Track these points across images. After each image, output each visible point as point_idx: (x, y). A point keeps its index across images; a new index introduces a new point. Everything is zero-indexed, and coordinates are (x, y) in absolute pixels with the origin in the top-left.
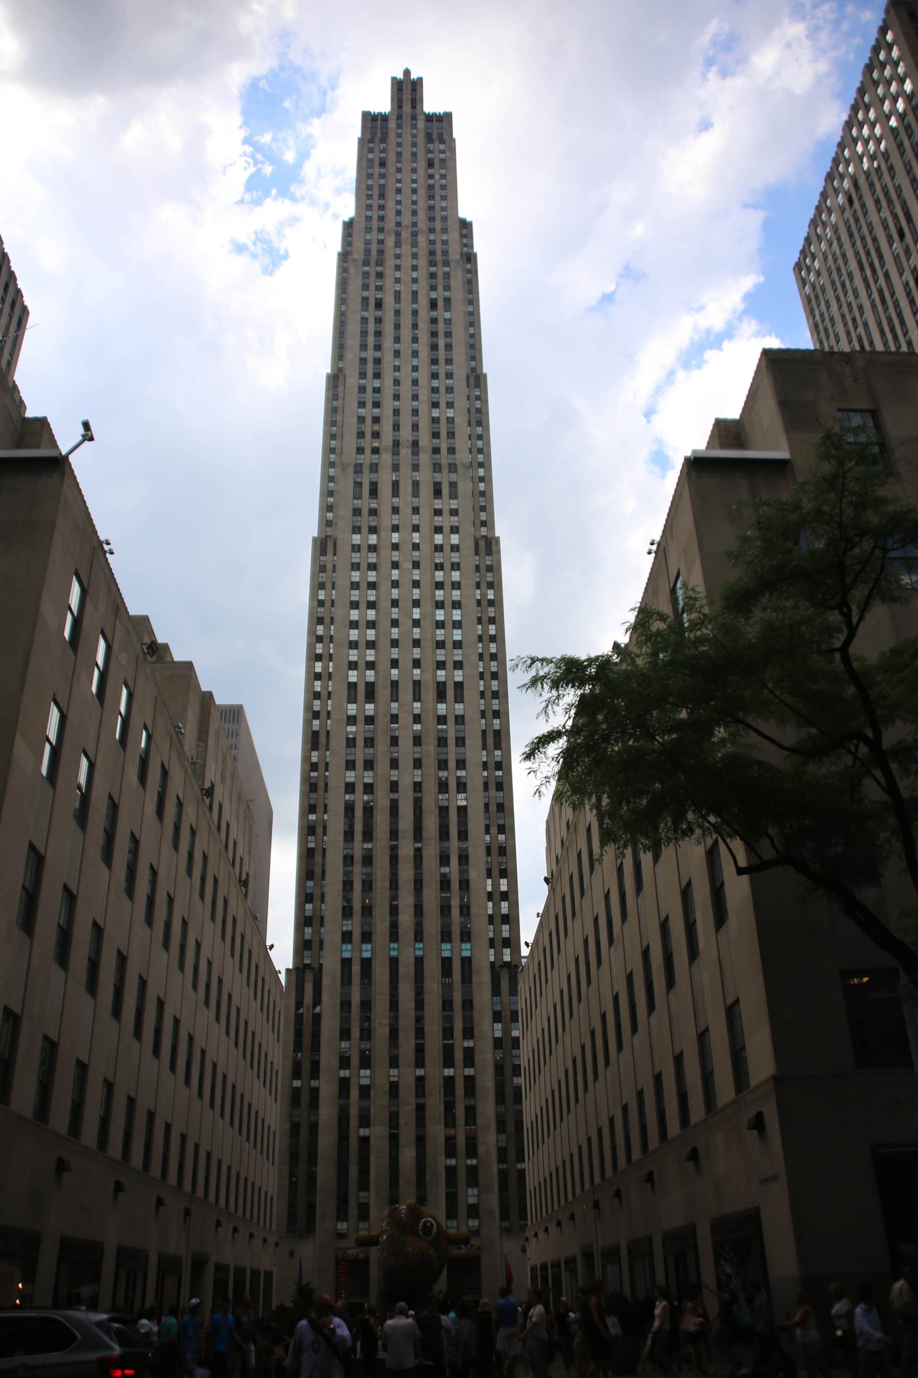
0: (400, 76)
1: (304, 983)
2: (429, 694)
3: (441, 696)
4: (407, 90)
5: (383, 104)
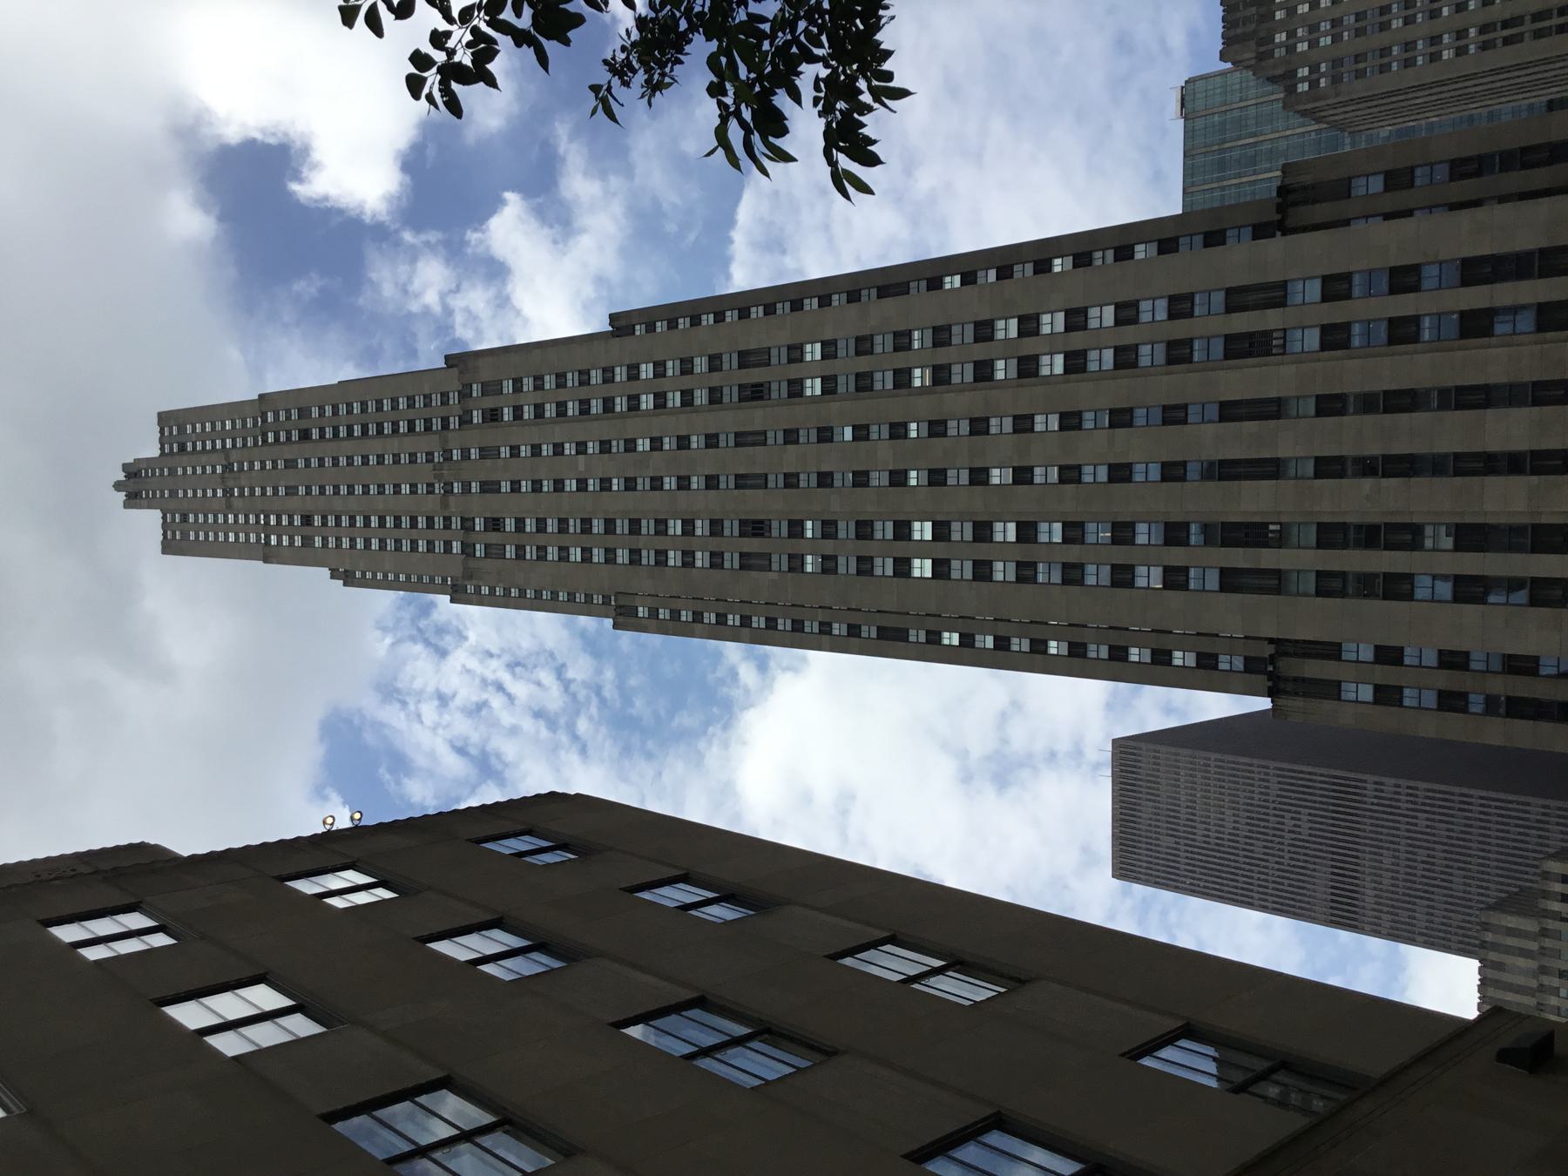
0: (122, 496)
1: (1304, 680)
2: (755, 417)
3: (755, 393)
4: (137, 485)
5: (150, 521)
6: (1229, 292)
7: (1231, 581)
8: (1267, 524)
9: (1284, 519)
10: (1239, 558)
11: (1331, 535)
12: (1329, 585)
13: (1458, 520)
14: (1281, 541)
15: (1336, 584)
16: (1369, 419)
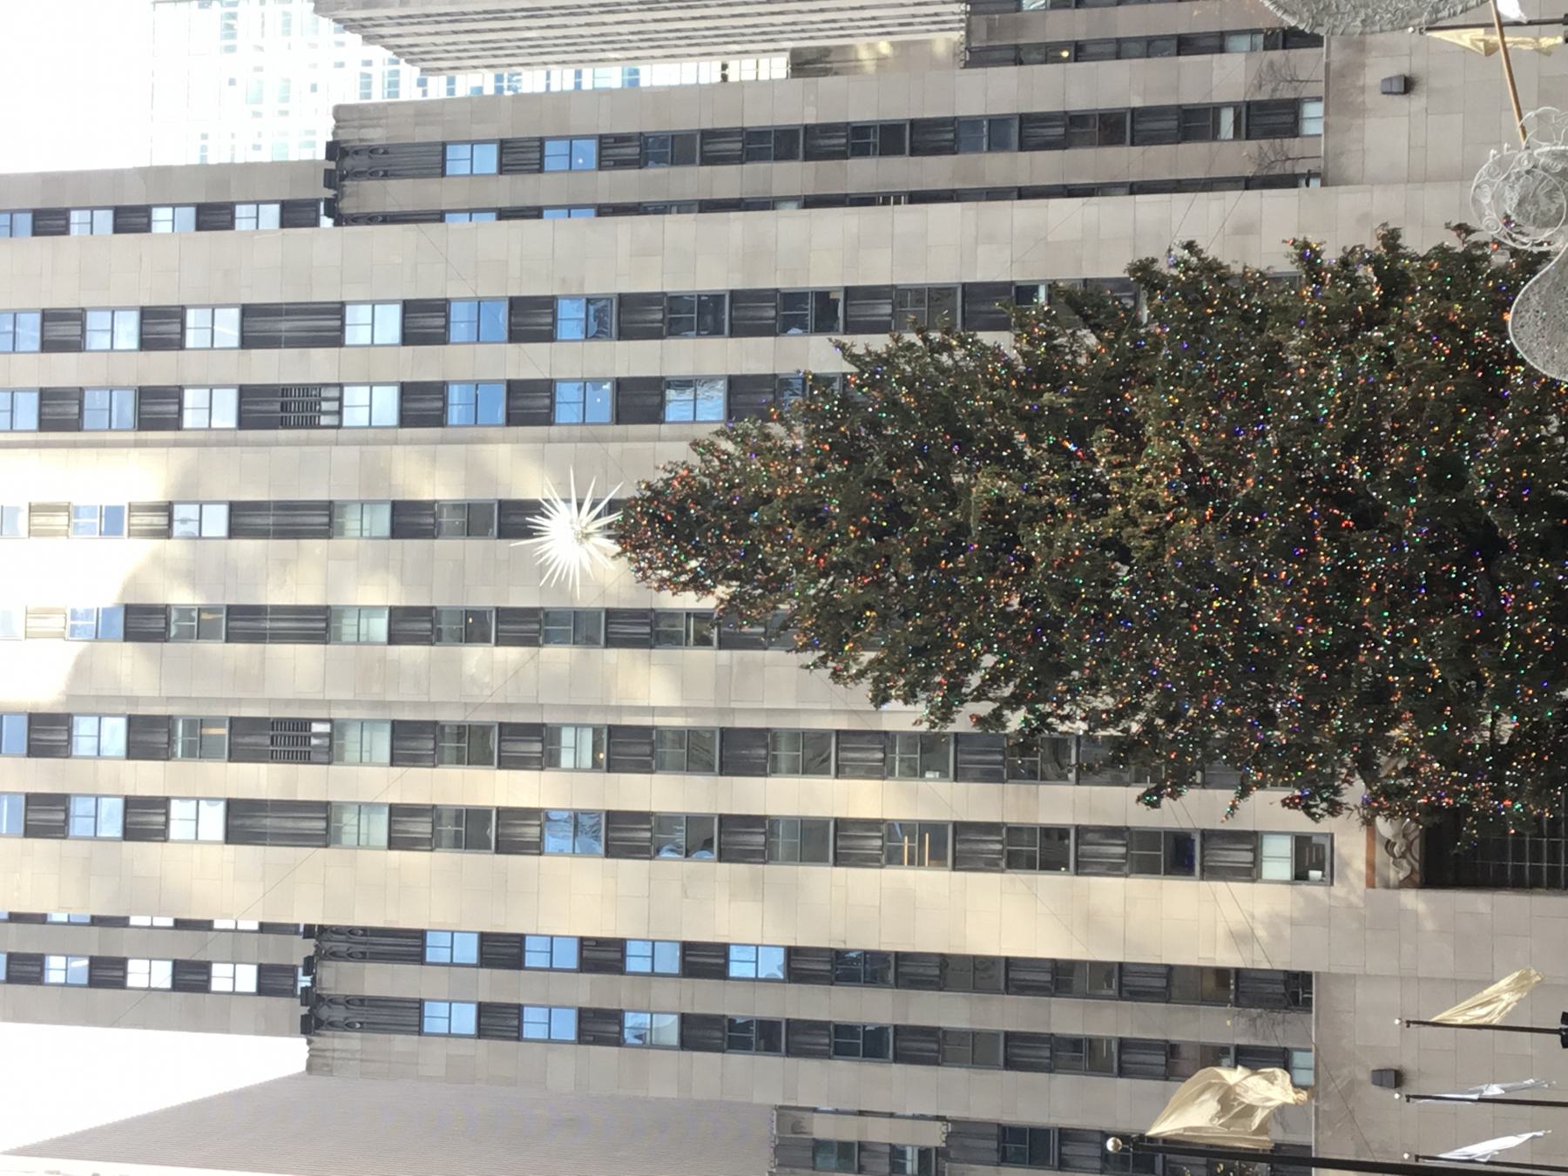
6: (247, 311)
7: (246, 822)
8: (310, 721)
9: (337, 714)
10: (262, 780)
11: (414, 741)
12: (408, 827)
13: (613, 720)
14: (330, 753)
15: (422, 828)
16: (475, 546)
